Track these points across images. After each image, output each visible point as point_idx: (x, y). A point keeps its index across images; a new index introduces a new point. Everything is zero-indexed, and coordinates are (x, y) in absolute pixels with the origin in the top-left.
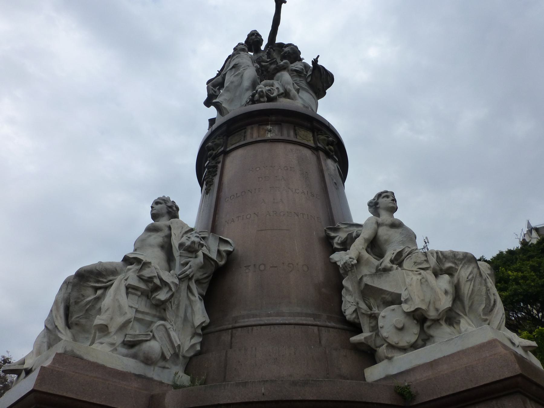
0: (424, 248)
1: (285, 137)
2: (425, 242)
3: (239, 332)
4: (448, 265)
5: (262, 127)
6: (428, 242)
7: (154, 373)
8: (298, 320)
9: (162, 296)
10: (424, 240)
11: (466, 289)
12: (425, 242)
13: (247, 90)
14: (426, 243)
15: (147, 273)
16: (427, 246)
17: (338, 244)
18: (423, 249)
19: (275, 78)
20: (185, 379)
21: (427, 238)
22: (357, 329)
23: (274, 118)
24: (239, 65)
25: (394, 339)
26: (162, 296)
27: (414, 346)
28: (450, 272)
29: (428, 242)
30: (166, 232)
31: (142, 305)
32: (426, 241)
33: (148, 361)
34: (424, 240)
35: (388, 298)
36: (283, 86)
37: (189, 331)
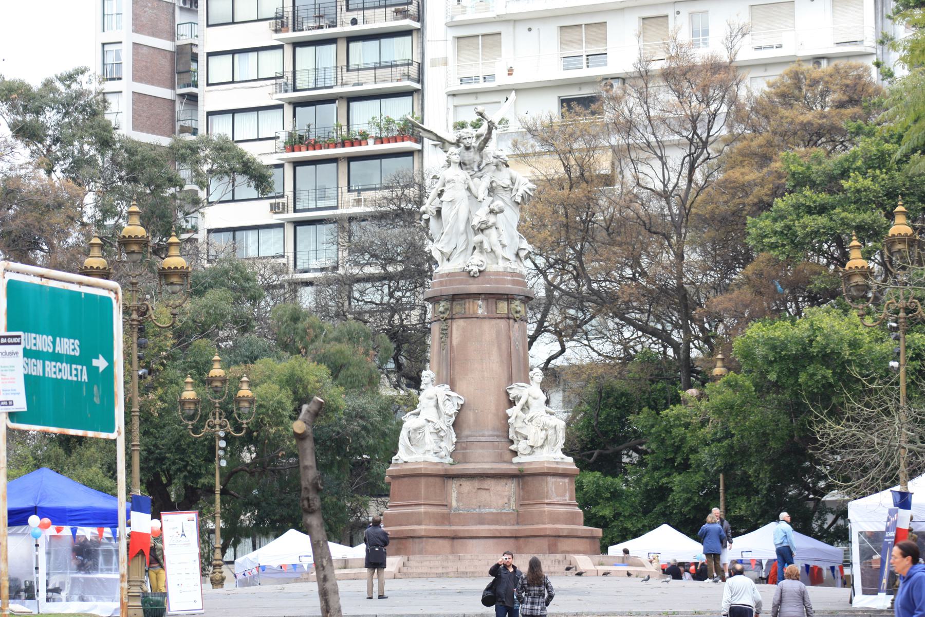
1: (490, 315)
3: (469, 443)
5: (476, 301)
7: (443, 461)
8: (491, 439)
9: (442, 434)
11: (549, 438)
13: (462, 234)
15: (437, 427)
20: (451, 460)
22: (512, 442)
23: (483, 296)
25: (522, 452)
26: (442, 434)
27: (529, 454)
28: (546, 430)
30: (435, 399)
31: (435, 437)
33: (442, 458)
36: (490, 243)
37: (451, 444)
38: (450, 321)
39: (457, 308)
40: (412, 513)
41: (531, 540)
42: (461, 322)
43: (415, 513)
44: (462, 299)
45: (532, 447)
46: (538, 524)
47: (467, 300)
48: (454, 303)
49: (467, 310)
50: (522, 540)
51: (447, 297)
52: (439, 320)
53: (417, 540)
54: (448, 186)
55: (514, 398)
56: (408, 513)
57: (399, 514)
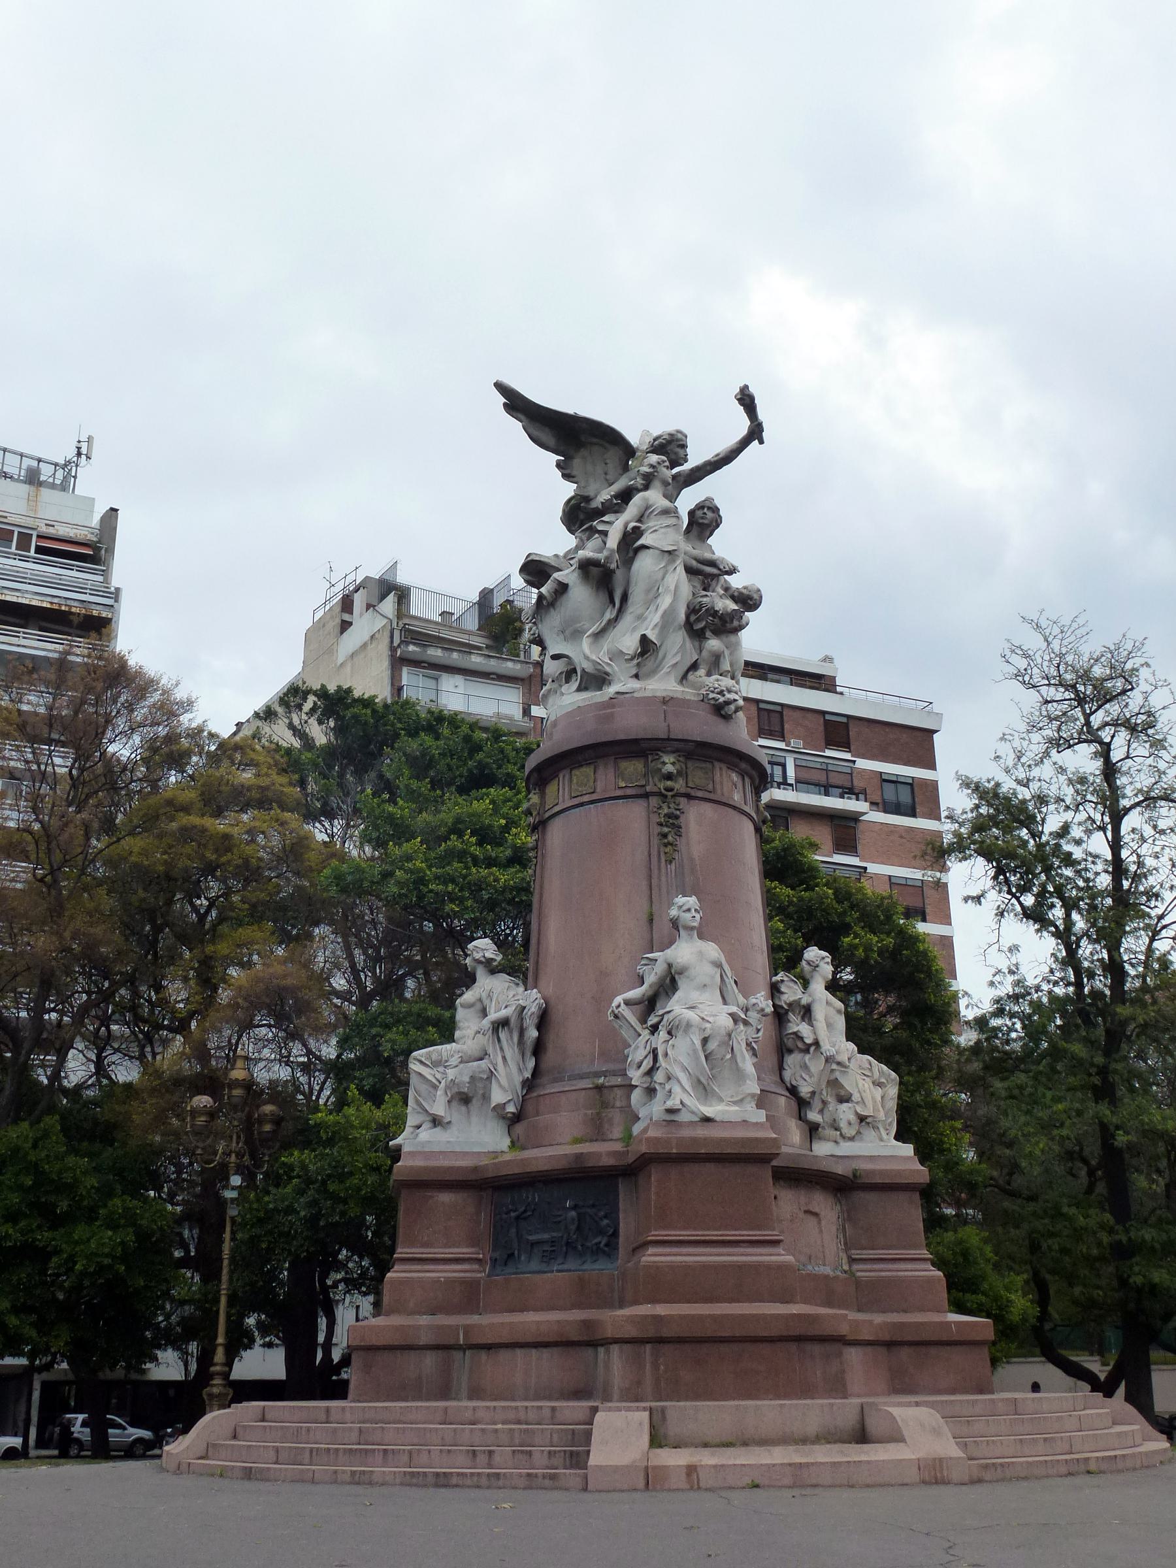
0: (68, 463)
2: (79, 448)
4: (883, 1080)
5: (730, 772)
6: (88, 458)
10: (79, 442)
12: (79, 448)
14: (79, 454)
16: (77, 466)
17: (786, 1003)
18: (56, 465)
19: (724, 637)
21: (90, 440)
23: (744, 765)
24: (676, 553)
29: (88, 458)
32: (84, 451)
34: (79, 442)
35: (843, 1093)
38: (683, 800)
39: (697, 776)
40: (756, 1268)
41: (933, 1351)
42: (707, 809)
43: (769, 1267)
44: (707, 759)
45: (862, 1119)
46: (922, 1309)
47: (717, 764)
48: (690, 764)
49: (718, 787)
50: (905, 1353)
51: (681, 745)
52: (646, 796)
53: (817, 1349)
54: (652, 523)
55: (790, 1005)
56: (740, 1268)
57: (705, 1267)
